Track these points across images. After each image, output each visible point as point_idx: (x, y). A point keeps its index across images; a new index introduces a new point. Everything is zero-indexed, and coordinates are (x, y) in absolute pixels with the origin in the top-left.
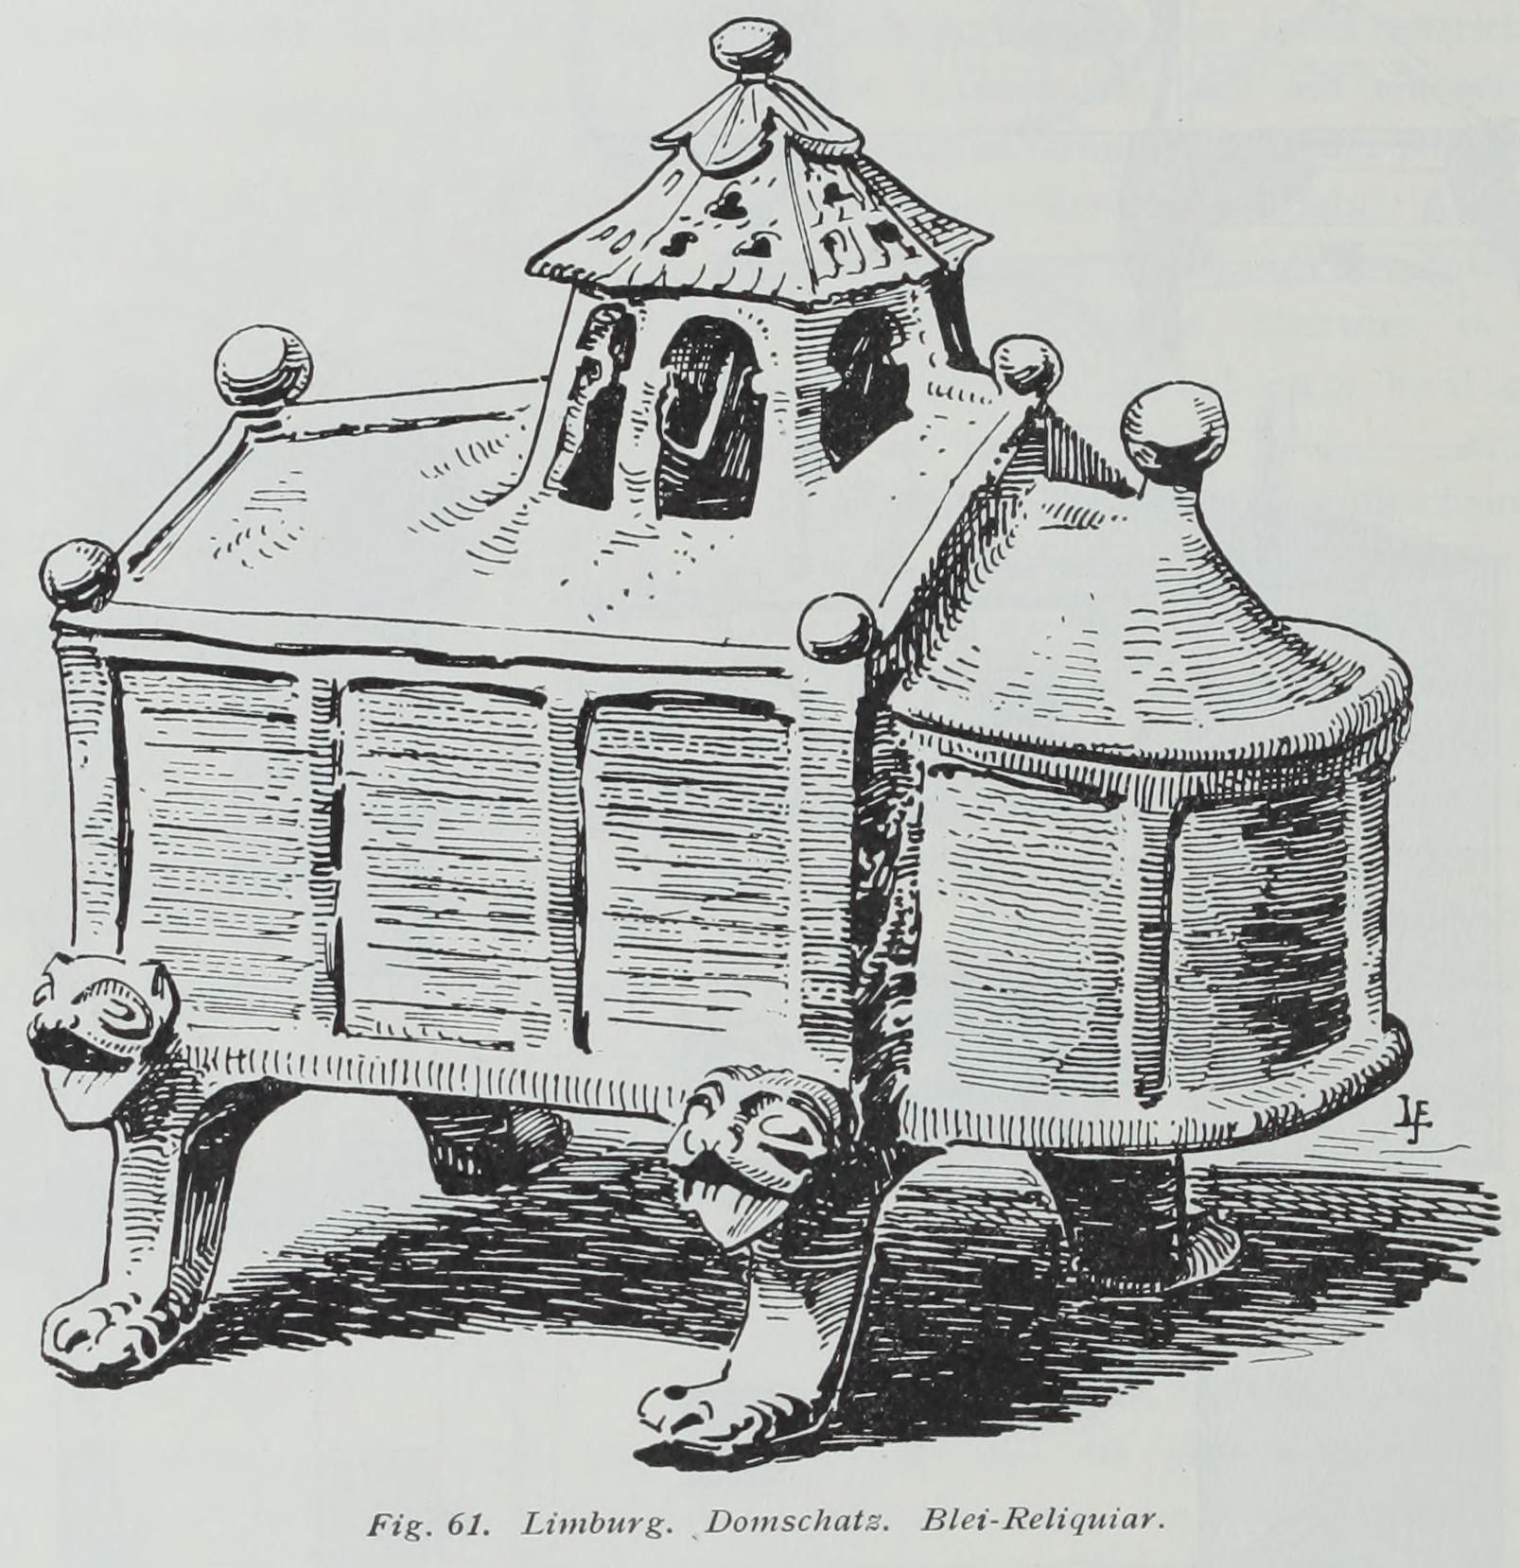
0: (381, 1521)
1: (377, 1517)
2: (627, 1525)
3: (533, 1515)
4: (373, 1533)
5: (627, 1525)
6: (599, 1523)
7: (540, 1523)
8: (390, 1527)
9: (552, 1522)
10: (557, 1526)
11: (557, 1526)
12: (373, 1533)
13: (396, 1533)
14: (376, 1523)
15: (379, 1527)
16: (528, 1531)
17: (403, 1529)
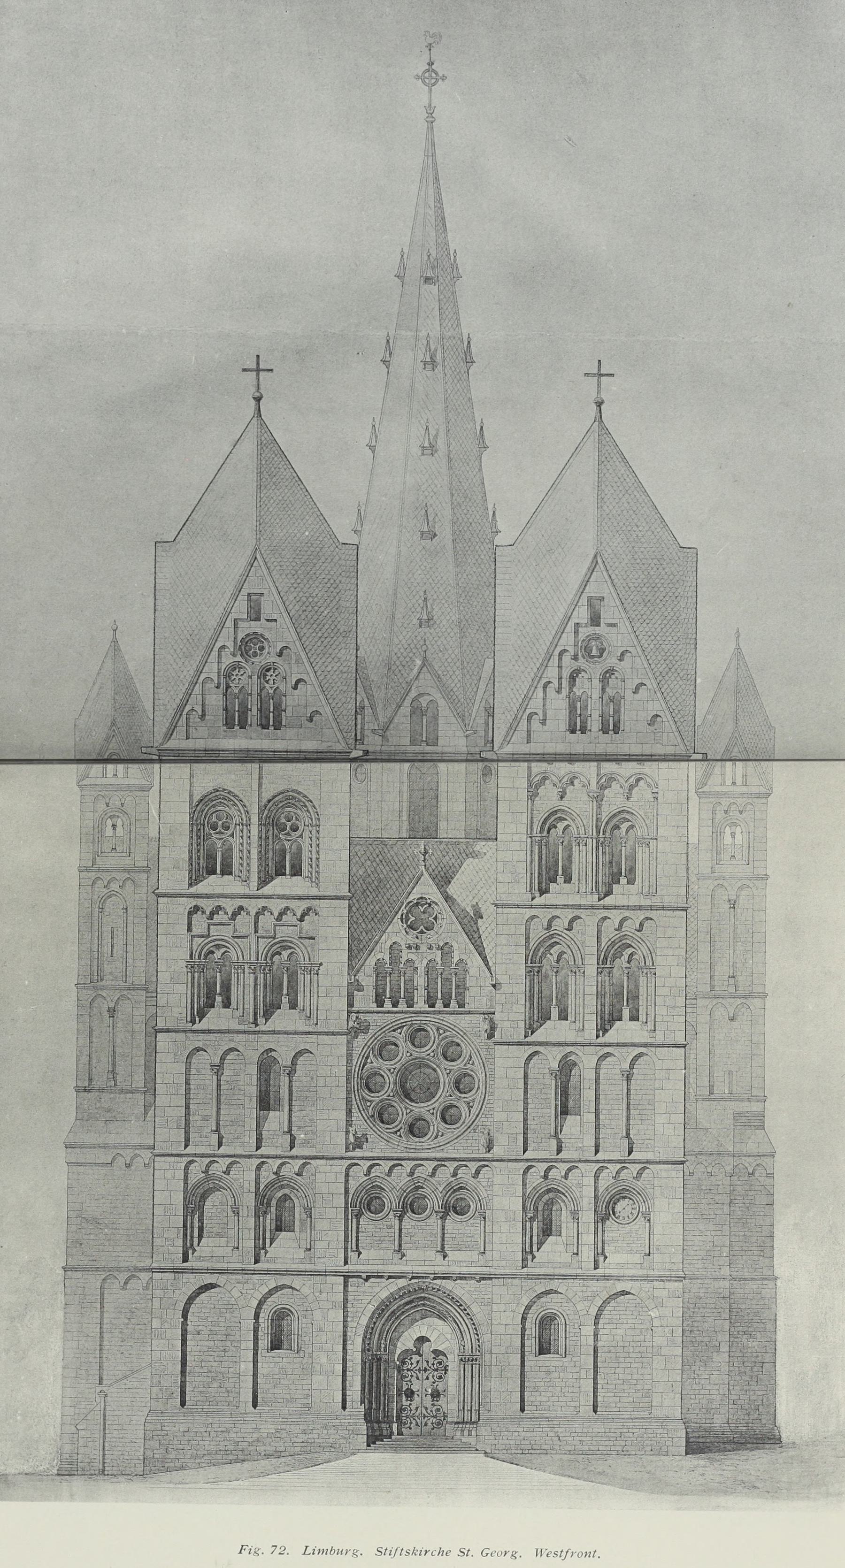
0: (244, 1547)
1: (242, 1546)
2: (344, 1552)
3: (307, 1547)
4: (240, 1552)
5: (344, 1552)
6: (333, 1551)
7: (309, 1550)
8: (247, 1551)
9: (314, 1550)
10: (316, 1552)
11: (316, 1552)
12: (240, 1552)
13: (249, 1553)
14: (242, 1549)
15: (243, 1551)
16: (304, 1554)
17: (252, 1551)
